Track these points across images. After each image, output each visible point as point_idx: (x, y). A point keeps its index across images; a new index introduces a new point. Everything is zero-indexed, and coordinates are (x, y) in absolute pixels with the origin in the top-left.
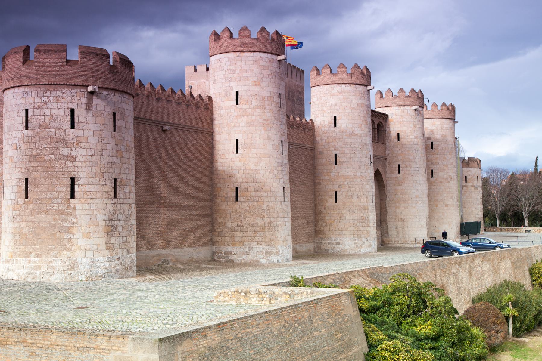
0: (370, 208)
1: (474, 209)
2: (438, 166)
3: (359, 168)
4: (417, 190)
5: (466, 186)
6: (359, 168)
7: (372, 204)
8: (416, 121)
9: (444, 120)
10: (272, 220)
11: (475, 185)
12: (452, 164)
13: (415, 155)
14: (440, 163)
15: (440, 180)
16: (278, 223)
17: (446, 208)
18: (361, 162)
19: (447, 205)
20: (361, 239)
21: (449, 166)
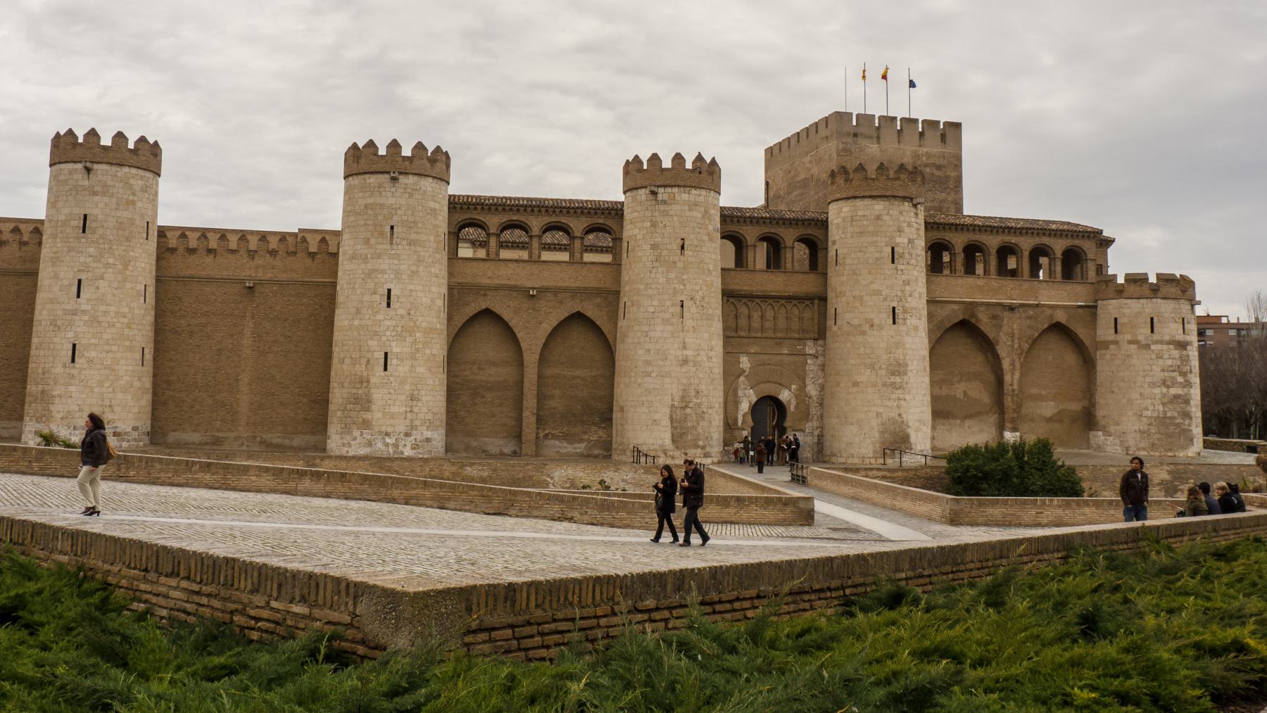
0: (373, 380)
1: (1135, 396)
2: (844, 299)
3: (358, 311)
4: (649, 351)
5: (1116, 343)
6: (358, 311)
7: (383, 373)
8: (657, 214)
9: (859, 203)
10: (46, 388)
11: (1140, 338)
12: (878, 293)
13: (650, 281)
14: (848, 293)
15: (846, 328)
16: (55, 393)
17: (855, 389)
18: (362, 302)
19: (856, 384)
20: (350, 432)
21: (866, 298)
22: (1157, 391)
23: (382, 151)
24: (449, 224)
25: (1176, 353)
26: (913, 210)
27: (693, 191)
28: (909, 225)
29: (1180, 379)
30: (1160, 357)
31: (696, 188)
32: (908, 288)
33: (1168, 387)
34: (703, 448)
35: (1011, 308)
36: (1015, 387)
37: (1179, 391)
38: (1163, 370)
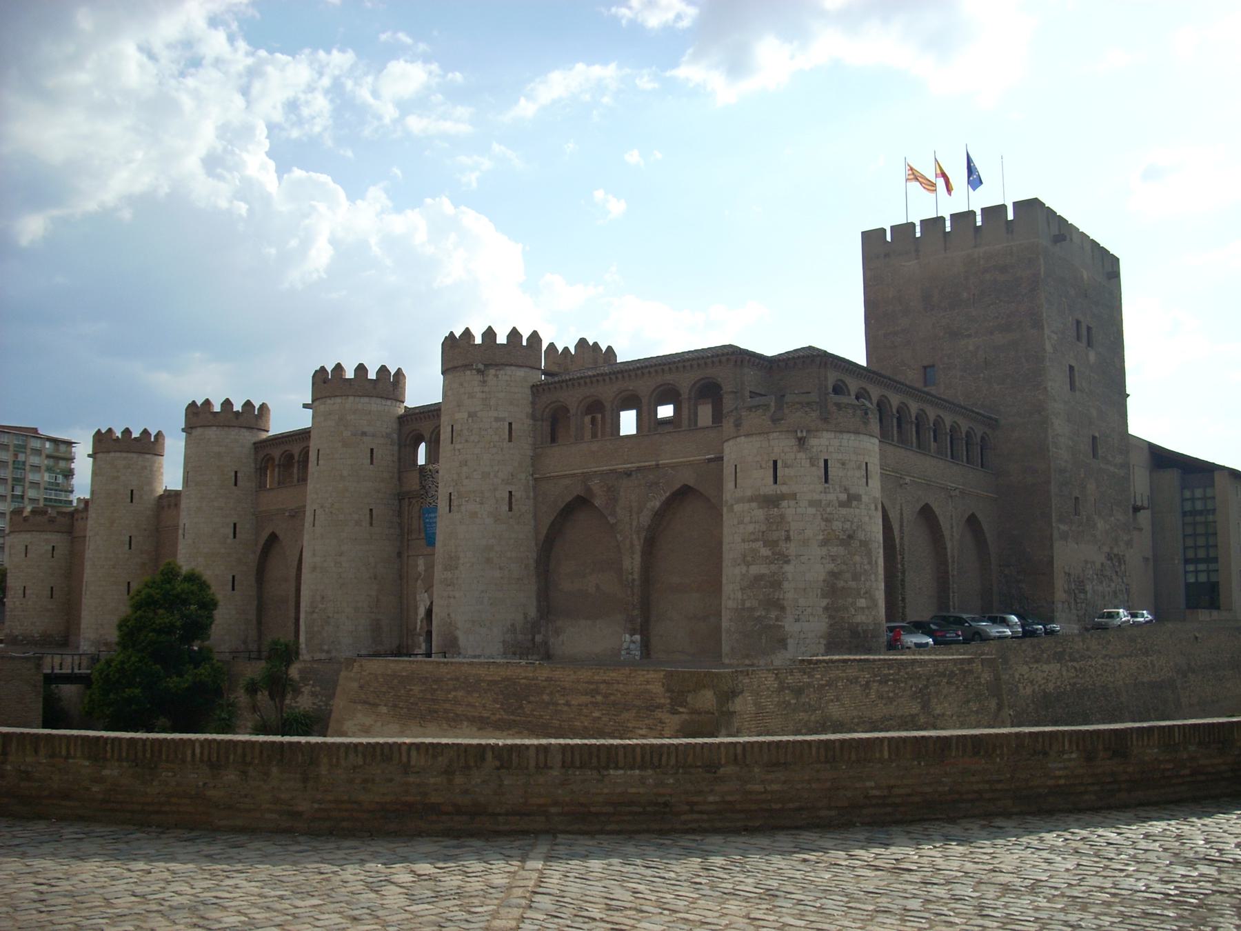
22: (737, 571)
23: (217, 408)
24: (256, 459)
25: (760, 514)
26: (480, 378)
27: (329, 401)
28: (471, 396)
29: (765, 552)
30: (741, 522)
31: (329, 397)
32: (465, 469)
33: (748, 565)
34: (328, 652)
35: (628, 474)
36: (636, 576)
37: (764, 570)
38: (743, 541)
